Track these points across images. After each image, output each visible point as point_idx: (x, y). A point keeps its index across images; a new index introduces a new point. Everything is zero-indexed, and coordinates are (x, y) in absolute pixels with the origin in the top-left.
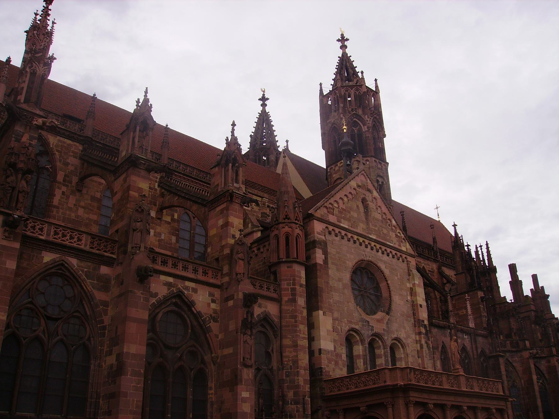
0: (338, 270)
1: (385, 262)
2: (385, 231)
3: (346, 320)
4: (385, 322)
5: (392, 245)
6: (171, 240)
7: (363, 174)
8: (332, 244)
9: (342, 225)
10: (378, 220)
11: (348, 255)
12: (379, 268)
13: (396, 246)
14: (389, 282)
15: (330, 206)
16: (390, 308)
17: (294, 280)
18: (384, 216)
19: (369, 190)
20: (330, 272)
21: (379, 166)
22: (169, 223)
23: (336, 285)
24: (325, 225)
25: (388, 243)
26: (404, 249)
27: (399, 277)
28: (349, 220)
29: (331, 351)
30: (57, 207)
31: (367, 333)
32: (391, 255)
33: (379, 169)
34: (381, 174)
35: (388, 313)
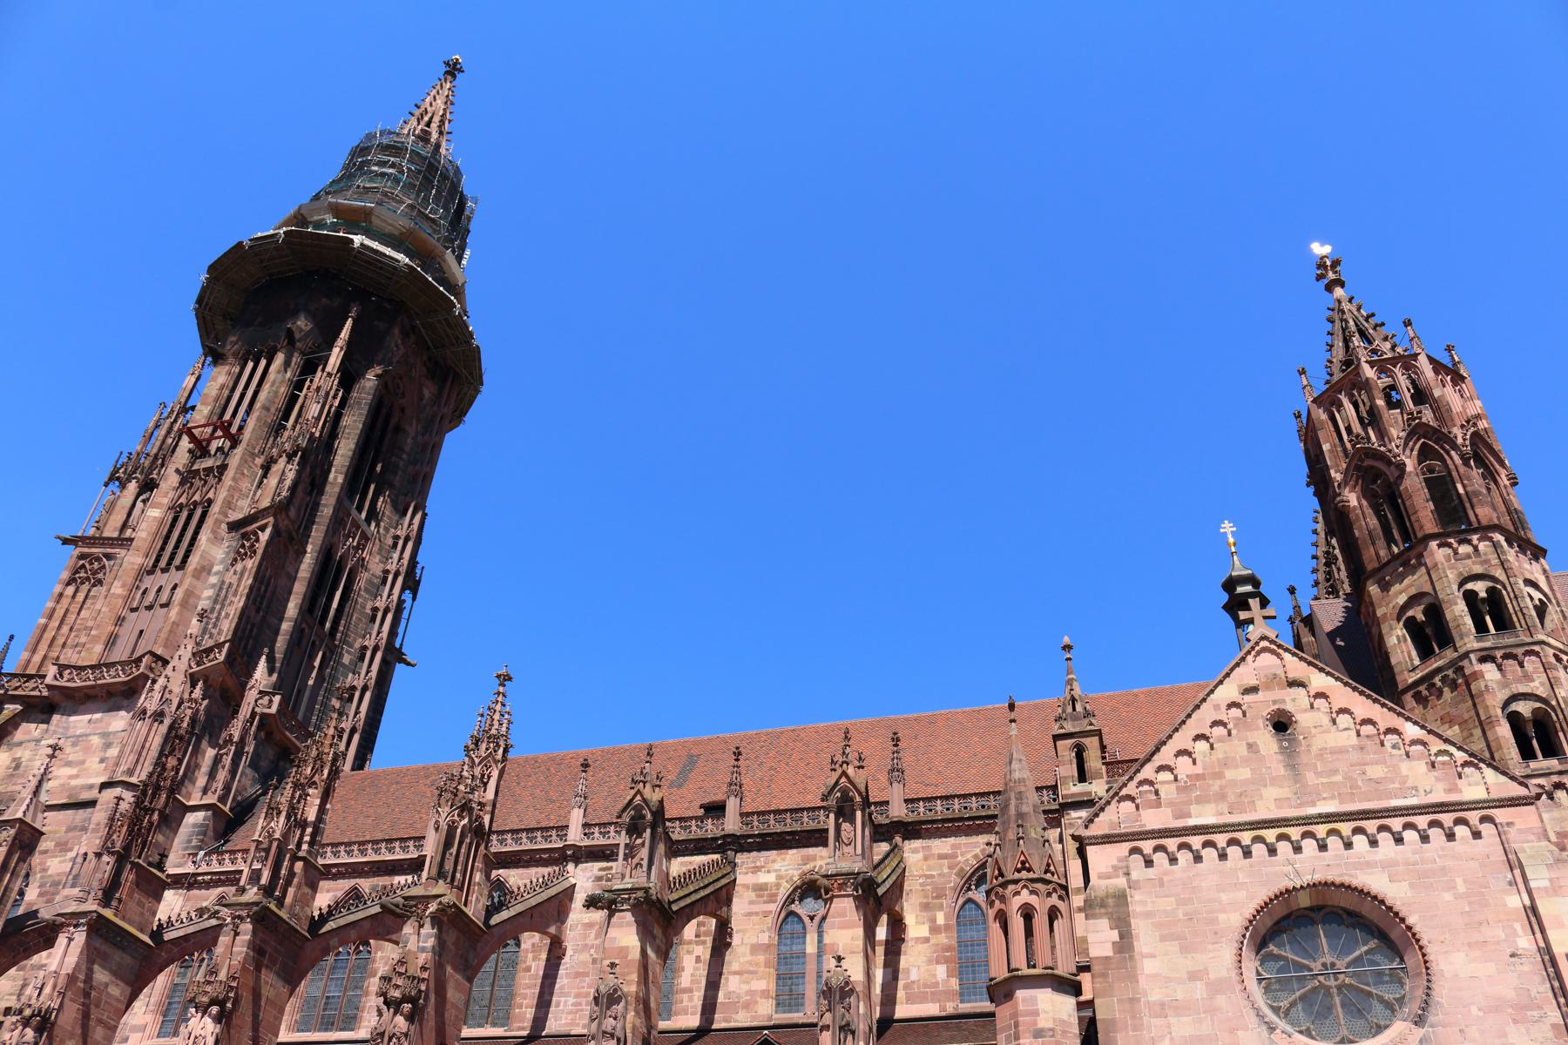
0: (1185, 950)
1: (1387, 865)
2: (1376, 772)
6: (934, 976)
7: (1265, 650)
8: (1161, 884)
9: (1192, 822)
10: (1341, 751)
11: (1224, 897)
13: (1439, 796)
14: (1410, 921)
15: (1146, 788)
16: (1426, 1004)
17: (1017, 1025)
18: (1367, 729)
19: (1294, 683)
20: (1148, 967)
21: (1464, 549)
22: (927, 940)
23: (1179, 996)
24: (1127, 846)
27: (1461, 888)
28: (1221, 797)
30: (690, 990)
32: (1410, 835)
33: (1468, 556)
34: (1478, 569)
35: (1419, 1021)
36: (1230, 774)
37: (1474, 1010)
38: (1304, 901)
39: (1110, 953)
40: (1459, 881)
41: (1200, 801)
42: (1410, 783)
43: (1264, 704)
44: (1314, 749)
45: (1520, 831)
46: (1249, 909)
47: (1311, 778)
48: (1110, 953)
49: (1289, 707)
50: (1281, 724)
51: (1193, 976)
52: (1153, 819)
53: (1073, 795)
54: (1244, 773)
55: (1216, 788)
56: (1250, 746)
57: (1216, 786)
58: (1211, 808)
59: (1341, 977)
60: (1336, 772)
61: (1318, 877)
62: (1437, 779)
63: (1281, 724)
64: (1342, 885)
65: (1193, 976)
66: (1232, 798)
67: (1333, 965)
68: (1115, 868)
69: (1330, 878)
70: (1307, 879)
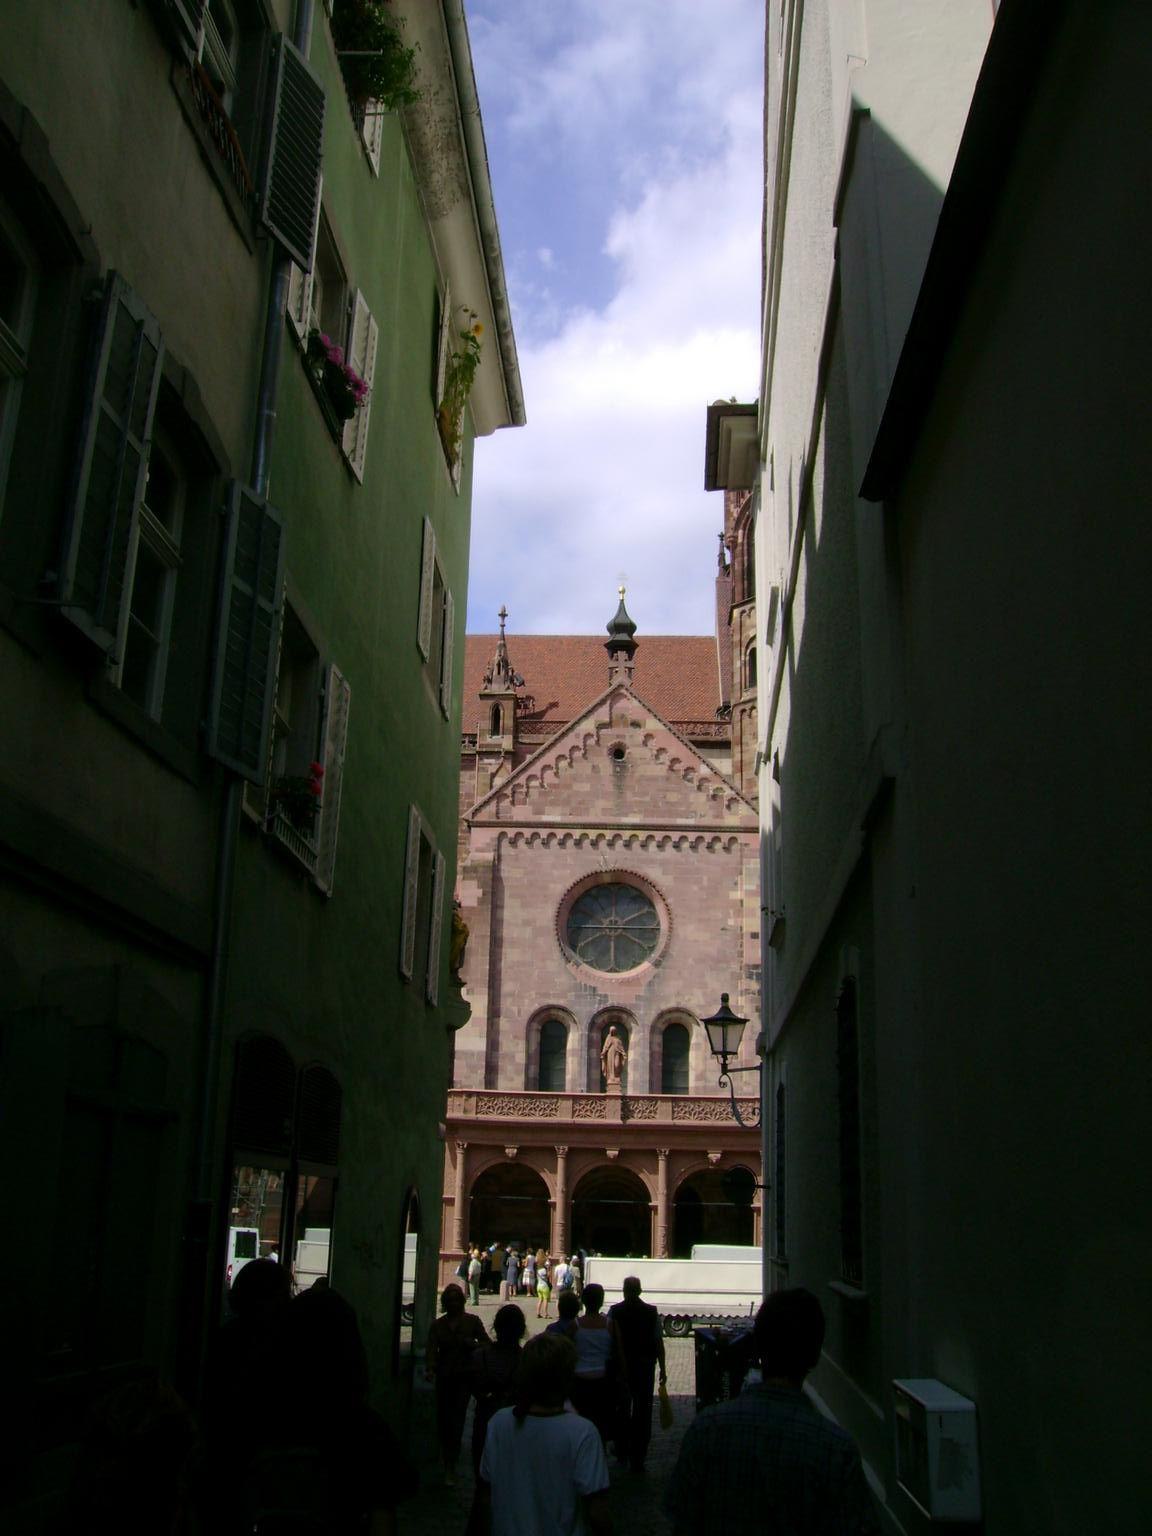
1: (663, 863)
2: (673, 797)
3: (533, 993)
4: (644, 982)
5: (691, 822)
9: (545, 818)
10: (654, 779)
11: (556, 873)
12: (644, 880)
19: (636, 724)
25: (681, 821)
26: (731, 820)
27: (705, 883)
28: (567, 802)
29: (479, 1053)
31: (584, 1010)
36: (577, 787)
37: (690, 961)
38: (607, 879)
39: (475, 904)
40: (705, 878)
41: (553, 803)
42: (693, 808)
43: (610, 737)
44: (637, 775)
45: (751, 850)
46: (569, 884)
47: (629, 796)
48: (475, 904)
49: (627, 741)
50: (618, 752)
51: (527, 923)
52: (520, 813)
53: (487, 745)
54: (586, 787)
55: (565, 795)
56: (594, 767)
57: (565, 794)
58: (559, 809)
59: (620, 931)
60: (645, 794)
61: (618, 866)
62: (711, 808)
63: (618, 752)
64: (632, 873)
65: (527, 923)
66: (574, 804)
67: (616, 922)
68: (488, 844)
69: (625, 867)
70: (611, 866)
